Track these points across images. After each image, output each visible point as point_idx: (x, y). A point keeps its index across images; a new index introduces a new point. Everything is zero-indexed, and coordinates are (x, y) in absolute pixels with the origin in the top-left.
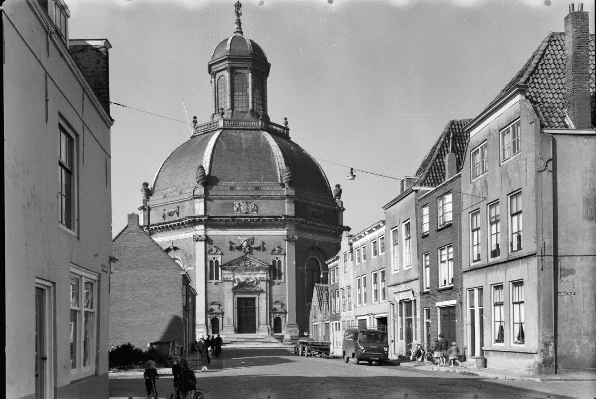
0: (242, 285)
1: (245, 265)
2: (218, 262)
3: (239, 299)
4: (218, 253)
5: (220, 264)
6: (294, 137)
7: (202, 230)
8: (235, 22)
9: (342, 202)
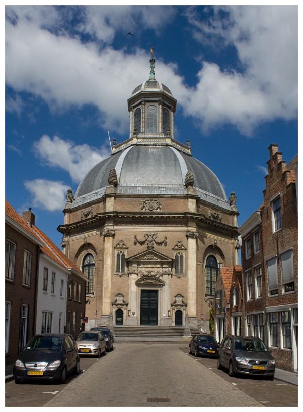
0: (145, 278)
2: (125, 256)
3: (142, 290)
4: (124, 246)
5: (126, 257)
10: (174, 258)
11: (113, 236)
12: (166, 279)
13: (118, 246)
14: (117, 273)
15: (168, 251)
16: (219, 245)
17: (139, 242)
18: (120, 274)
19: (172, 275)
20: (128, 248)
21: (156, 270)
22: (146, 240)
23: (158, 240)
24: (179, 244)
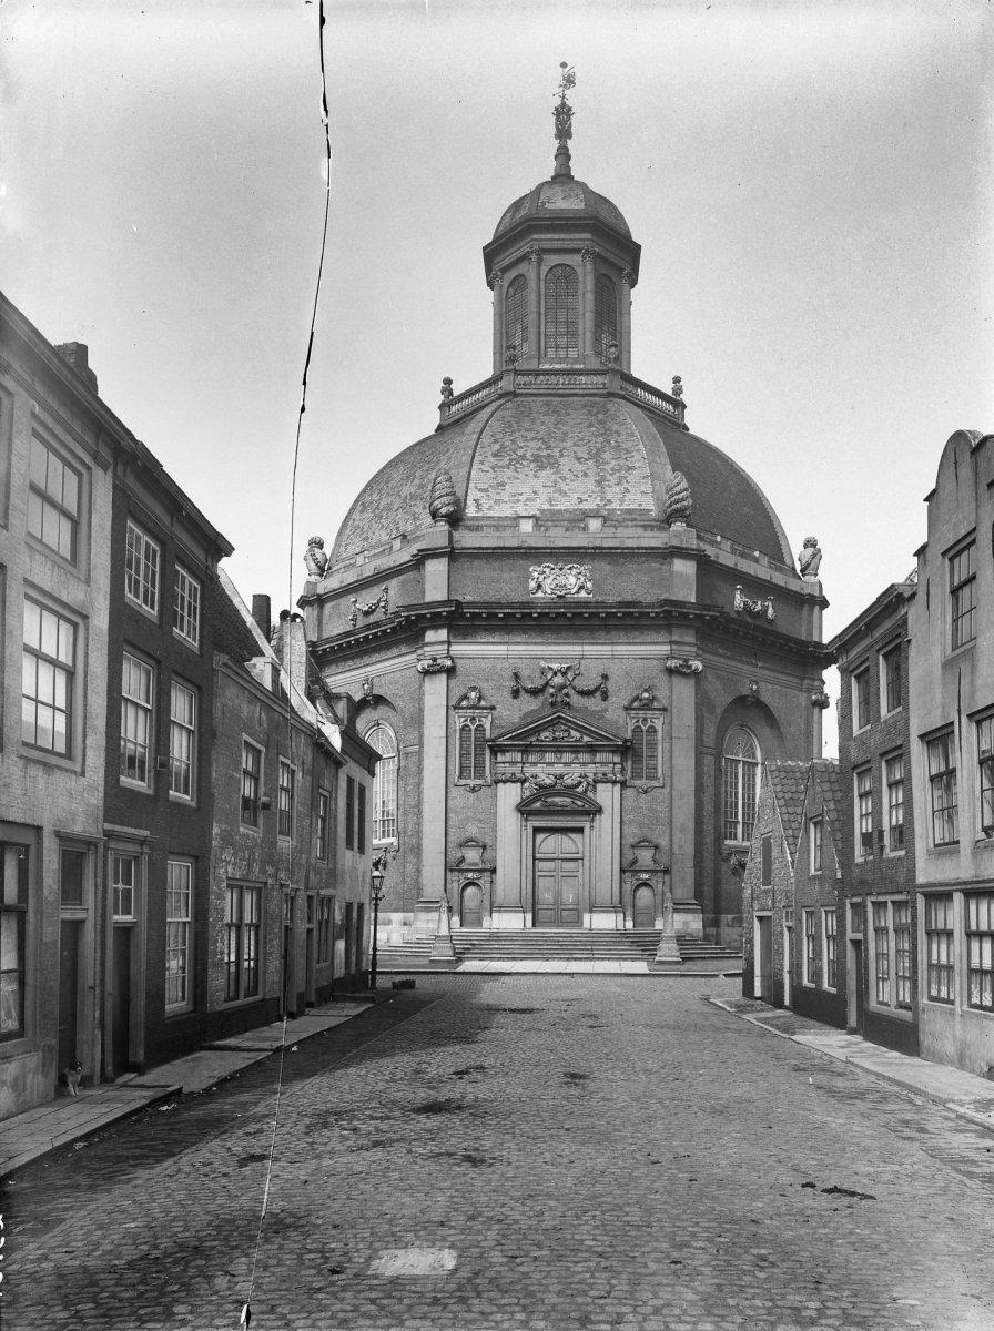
0: (544, 791)
1: (555, 739)
4: (483, 703)
5: (488, 735)
6: (698, 422)
7: (442, 643)
8: (554, 152)
9: (821, 585)
10: (629, 735)
11: (450, 672)
12: (606, 795)
13: (464, 703)
14: (463, 782)
15: (615, 715)
16: (766, 697)
17: (527, 691)
18: (471, 782)
19: (624, 784)
20: (493, 708)
21: (573, 770)
22: (547, 684)
23: (581, 684)
24: (646, 695)
